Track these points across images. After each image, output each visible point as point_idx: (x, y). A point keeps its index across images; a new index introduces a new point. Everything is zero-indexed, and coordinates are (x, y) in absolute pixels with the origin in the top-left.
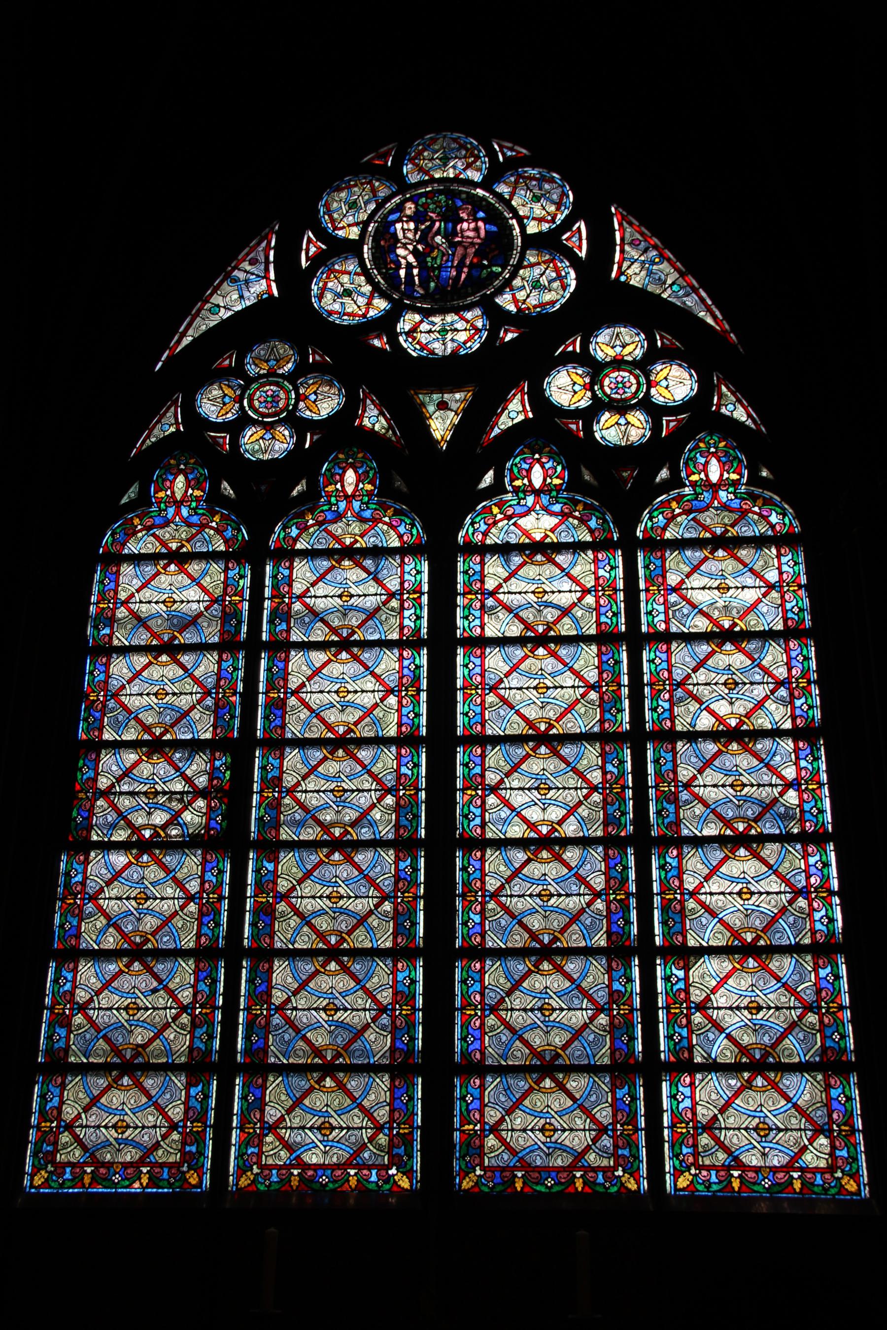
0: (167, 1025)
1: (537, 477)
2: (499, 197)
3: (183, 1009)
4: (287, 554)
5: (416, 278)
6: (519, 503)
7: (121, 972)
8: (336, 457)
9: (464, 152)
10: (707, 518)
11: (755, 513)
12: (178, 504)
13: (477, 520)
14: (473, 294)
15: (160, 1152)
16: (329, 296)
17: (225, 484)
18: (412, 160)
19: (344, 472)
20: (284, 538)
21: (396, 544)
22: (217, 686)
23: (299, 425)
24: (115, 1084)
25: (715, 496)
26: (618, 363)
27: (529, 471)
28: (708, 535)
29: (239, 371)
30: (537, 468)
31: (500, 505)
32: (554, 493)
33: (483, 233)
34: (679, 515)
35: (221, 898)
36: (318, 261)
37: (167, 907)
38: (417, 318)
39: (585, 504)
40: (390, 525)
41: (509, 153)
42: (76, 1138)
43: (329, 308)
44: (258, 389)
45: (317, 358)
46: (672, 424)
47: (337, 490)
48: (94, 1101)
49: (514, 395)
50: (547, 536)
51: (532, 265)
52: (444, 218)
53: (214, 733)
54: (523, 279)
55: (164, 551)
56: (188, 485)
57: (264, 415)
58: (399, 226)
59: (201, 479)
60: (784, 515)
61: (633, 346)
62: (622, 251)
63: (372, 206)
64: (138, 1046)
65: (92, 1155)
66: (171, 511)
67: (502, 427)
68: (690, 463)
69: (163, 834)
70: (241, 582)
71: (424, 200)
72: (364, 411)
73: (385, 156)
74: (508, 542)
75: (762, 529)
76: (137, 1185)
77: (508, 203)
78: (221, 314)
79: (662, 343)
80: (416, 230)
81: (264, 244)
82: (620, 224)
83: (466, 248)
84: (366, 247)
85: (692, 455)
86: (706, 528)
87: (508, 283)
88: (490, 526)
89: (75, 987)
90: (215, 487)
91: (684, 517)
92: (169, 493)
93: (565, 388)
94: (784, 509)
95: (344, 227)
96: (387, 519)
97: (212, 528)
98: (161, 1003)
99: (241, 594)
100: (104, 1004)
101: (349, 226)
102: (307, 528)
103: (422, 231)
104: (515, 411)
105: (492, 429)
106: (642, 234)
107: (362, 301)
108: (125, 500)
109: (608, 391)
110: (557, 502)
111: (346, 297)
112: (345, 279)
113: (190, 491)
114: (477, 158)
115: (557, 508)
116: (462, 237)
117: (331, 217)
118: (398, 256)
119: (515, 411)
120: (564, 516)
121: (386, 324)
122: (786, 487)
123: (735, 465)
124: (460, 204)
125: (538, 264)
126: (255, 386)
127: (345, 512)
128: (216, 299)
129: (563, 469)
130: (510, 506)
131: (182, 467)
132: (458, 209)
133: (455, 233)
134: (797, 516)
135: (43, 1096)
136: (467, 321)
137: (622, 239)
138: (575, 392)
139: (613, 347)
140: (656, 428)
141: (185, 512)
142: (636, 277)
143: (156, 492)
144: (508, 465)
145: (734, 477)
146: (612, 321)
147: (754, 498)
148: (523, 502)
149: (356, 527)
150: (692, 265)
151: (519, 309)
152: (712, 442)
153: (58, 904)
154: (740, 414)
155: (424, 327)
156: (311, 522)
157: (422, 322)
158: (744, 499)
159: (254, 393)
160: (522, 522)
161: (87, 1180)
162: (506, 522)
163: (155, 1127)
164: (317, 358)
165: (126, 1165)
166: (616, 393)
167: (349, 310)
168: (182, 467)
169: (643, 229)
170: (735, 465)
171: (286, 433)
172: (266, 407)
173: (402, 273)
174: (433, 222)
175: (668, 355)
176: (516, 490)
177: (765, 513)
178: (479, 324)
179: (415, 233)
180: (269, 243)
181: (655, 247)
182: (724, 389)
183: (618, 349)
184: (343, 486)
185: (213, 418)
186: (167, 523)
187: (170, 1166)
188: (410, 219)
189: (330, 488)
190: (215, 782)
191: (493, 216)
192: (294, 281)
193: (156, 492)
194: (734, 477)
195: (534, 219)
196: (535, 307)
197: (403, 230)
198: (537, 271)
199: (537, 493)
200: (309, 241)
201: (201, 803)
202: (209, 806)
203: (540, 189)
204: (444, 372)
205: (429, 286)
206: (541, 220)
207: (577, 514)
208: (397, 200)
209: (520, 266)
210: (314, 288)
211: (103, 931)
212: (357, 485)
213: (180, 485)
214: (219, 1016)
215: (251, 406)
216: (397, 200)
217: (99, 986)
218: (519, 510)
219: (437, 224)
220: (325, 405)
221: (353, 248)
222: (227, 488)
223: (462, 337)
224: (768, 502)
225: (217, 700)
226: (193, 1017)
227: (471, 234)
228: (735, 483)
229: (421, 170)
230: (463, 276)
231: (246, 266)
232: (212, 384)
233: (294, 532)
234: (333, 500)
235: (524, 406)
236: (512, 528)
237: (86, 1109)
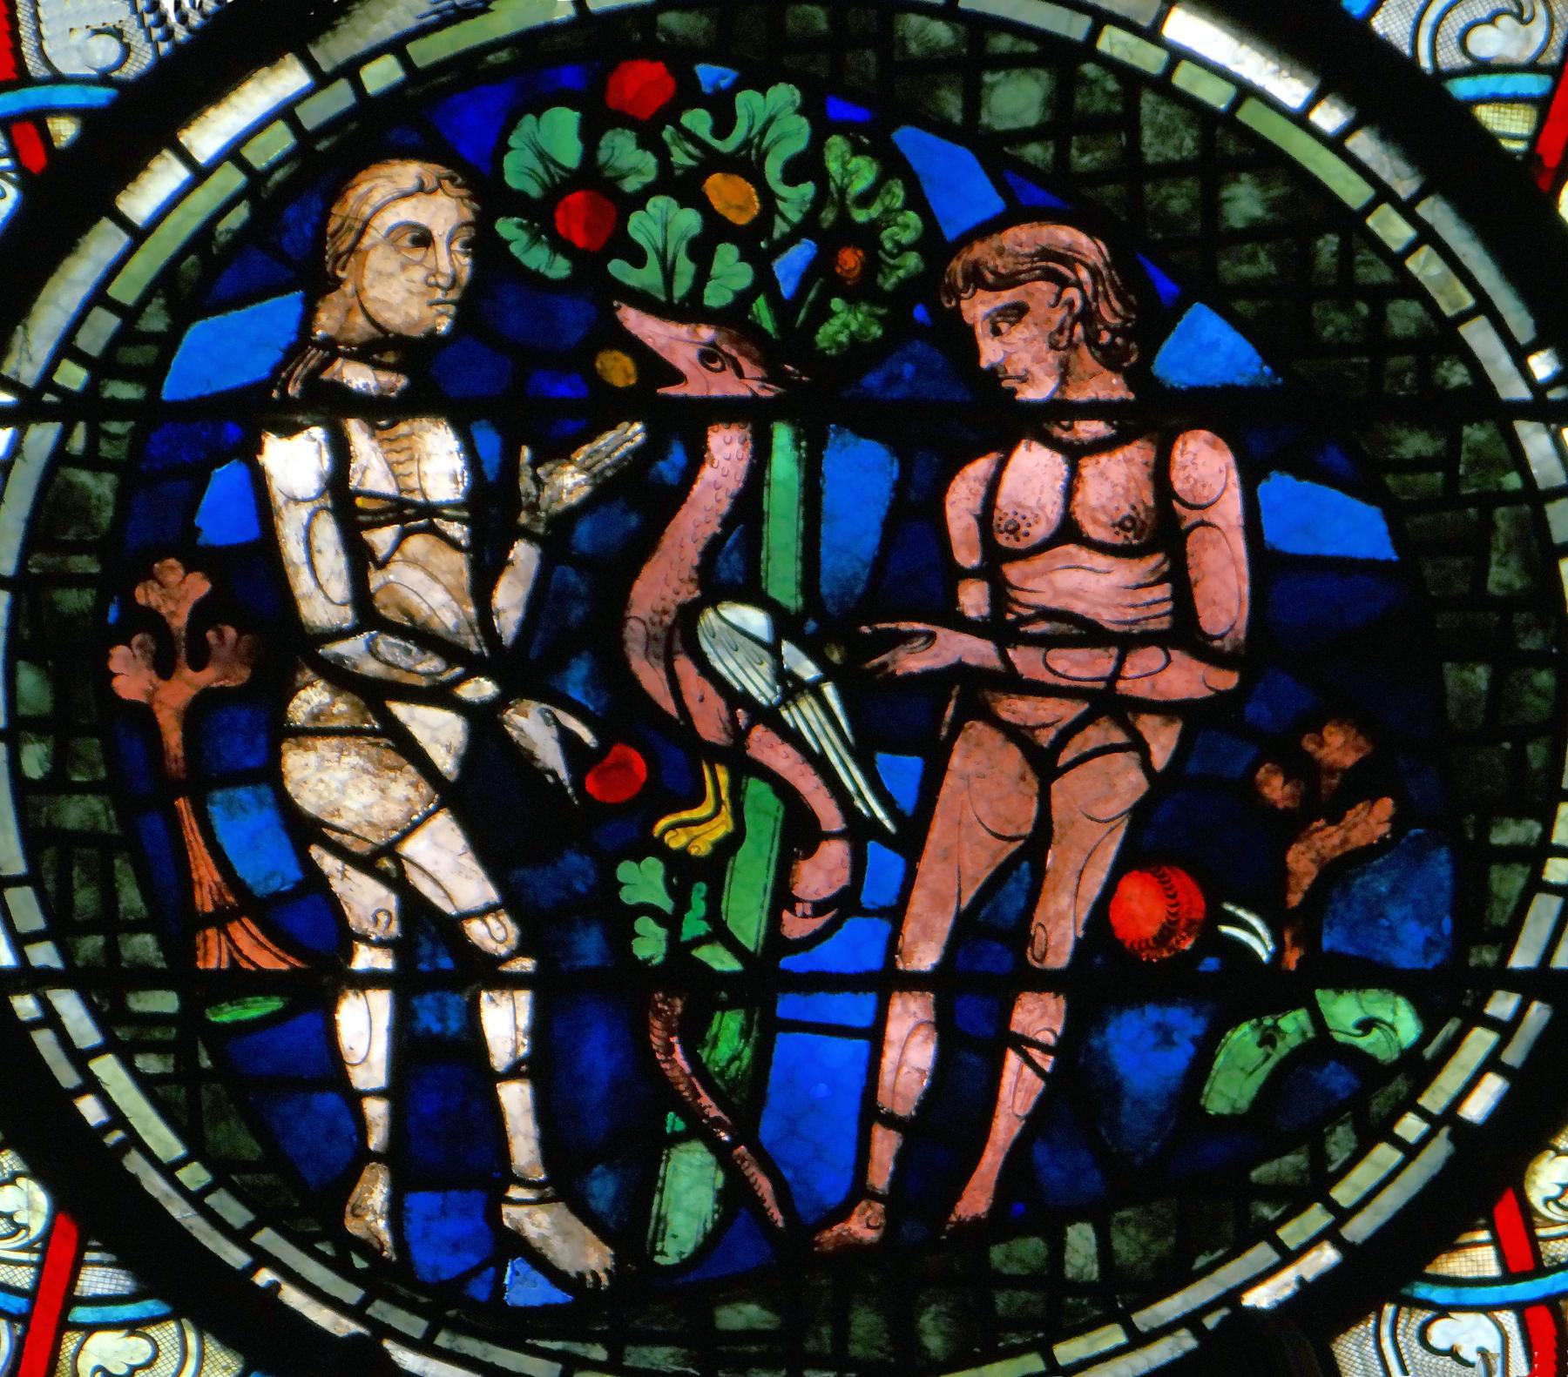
5: (515, 1098)
33: (1225, 591)
52: (813, 395)
58: (294, 462)
71: (558, 133)
80: (491, 514)
83: (1045, 764)
103: (557, 536)
116: (1001, 627)
118: (305, 830)
124: (968, 192)
173: (364, 1028)
174: (686, 426)
179: (486, 570)
188: (430, 377)
205: (643, 1186)
219: (727, 449)
227: (1096, 586)
230: (1018, 1088)
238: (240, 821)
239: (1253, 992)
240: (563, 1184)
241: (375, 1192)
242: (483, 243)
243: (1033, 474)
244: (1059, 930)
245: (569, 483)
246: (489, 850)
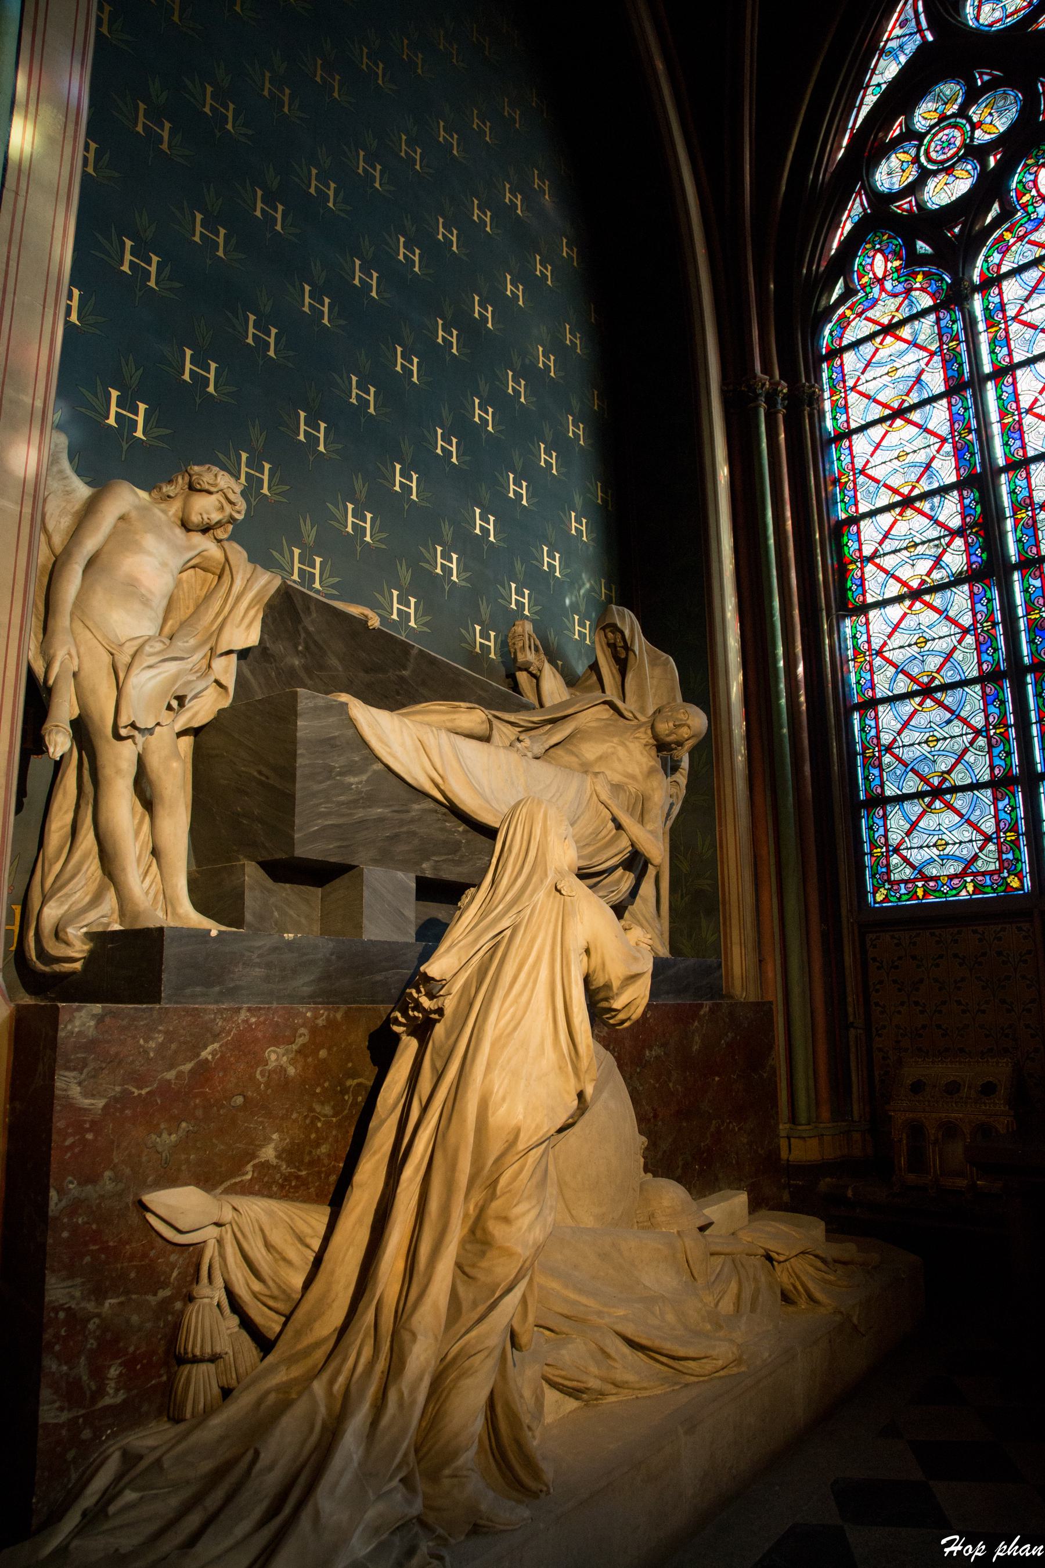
0: (965, 751)
3: (978, 732)
4: (992, 281)
7: (916, 711)
8: (1026, 165)
12: (881, 281)
15: (979, 863)
17: (920, 244)
20: (988, 269)
22: (952, 430)
24: (928, 809)
35: (994, 625)
37: (944, 645)
42: (905, 860)
44: (932, 140)
48: (914, 825)
53: (958, 475)
56: (886, 260)
64: (943, 772)
65: (920, 872)
66: (876, 290)
69: (929, 581)
70: (955, 327)
76: (964, 893)
89: (878, 732)
90: (911, 248)
98: (957, 731)
99: (956, 338)
100: (907, 741)
126: (928, 138)
135: (870, 828)
153: (851, 663)
156: (1012, 241)
161: (920, 893)
163: (971, 841)
165: (951, 877)
186: (875, 302)
187: (991, 873)
190: (968, 520)
201: (959, 542)
202: (966, 543)
211: (893, 680)
214: (1012, 732)
215: (930, 159)
217: (899, 726)
222: (922, 247)
225: (954, 443)
226: (989, 738)
233: (996, 257)
237: (908, 833)
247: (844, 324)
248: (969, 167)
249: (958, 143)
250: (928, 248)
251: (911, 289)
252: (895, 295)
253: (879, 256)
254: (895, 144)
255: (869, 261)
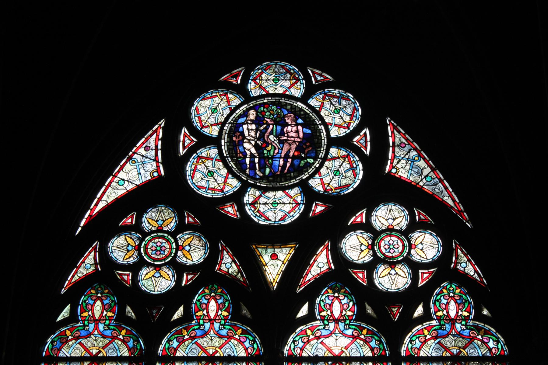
1: (337, 311)
2: (312, 108)
5: (257, 165)
6: (324, 328)
9: (289, 76)
10: (448, 342)
11: (479, 340)
13: (297, 339)
14: (295, 178)
16: (198, 175)
17: (128, 309)
18: (254, 80)
19: (209, 302)
20: (168, 348)
21: (243, 354)
23: (180, 269)
25: (453, 327)
26: (390, 231)
27: (331, 305)
28: (448, 354)
29: (137, 227)
30: (336, 303)
31: (312, 329)
32: (347, 322)
33: (301, 135)
34: (430, 339)
36: (192, 150)
38: (258, 193)
39: (368, 330)
40: (239, 341)
41: (319, 78)
43: (199, 184)
44: (150, 241)
45: (191, 220)
46: (425, 276)
47: (204, 315)
49: (322, 251)
50: (343, 352)
51: (333, 159)
52: (276, 123)
54: (328, 168)
55: (87, 355)
57: (155, 260)
58: (245, 127)
59: (113, 304)
60: (498, 342)
61: (400, 219)
62: (394, 152)
63: (227, 112)
67: (314, 273)
68: (437, 303)
71: (262, 109)
72: (222, 259)
73: (236, 76)
74: (317, 356)
75: (483, 351)
77: (318, 113)
78: (125, 185)
79: (420, 218)
80: (257, 130)
81: (154, 136)
82: (393, 132)
83: (290, 145)
84: (223, 141)
85: (438, 298)
86: (447, 349)
87: (318, 170)
88: (305, 343)
91: (433, 341)
92: (90, 313)
93: (355, 246)
94: (498, 338)
95: (208, 126)
96: (237, 337)
97: (120, 339)
101: (212, 125)
102: (184, 341)
104: (321, 262)
105: (307, 275)
106: (407, 140)
107: (221, 180)
108: (60, 318)
109: (383, 250)
110: (350, 328)
111: (208, 176)
112: (209, 163)
113: (105, 313)
114: (298, 80)
115: (349, 332)
116: (287, 137)
117: (199, 117)
118: (244, 148)
119: (321, 262)
120: (354, 338)
121: (237, 198)
122: (500, 323)
123: (466, 306)
124: (286, 112)
125: (338, 158)
126: (148, 238)
127: (209, 330)
128: (122, 175)
129: (354, 305)
130: (319, 330)
131: (99, 295)
132: (285, 116)
133: (282, 133)
134: (507, 343)
136: (291, 197)
137: (394, 143)
138: (362, 251)
139: (387, 220)
140: (415, 278)
141: (101, 327)
142: (403, 172)
143: (81, 313)
144: (318, 301)
145: (466, 314)
146: (386, 200)
147: (478, 329)
148: (327, 327)
149: (217, 342)
150: (439, 163)
151: (326, 190)
152: (451, 289)
154: (470, 270)
155: (262, 200)
156: (186, 337)
157: (260, 196)
158: (472, 330)
159: (148, 243)
160: (326, 341)
162: (316, 341)
164: (191, 220)
166: (390, 252)
167: (212, 186)
168: (99, 295)
169: (407, 136)
170: (466, 306)
171: (170, 273)
172: (156, 254)
173: (248, 160)
174: (269, 125)
175: (423, 226)
176: (323, 319)
177: (485, 340)
178: (299, 199)
180: (158, 136)
181: (415, 149)
182: (459, 251)
183: (390, 221)
184: (208, 312)
185: (120, 260)
188: (253, 122)
189: (199, 313)
191: (308, 123)
192: (174, 163)
193: (81, 313)
194: (466, 314)
195: (335, 125)
196: (336, 189)
197: (248, 130)
198: (337, 162)
199: (337, 321)
200: (185, 135)
203: (340, 104)
204: (276, 235)
205: (265, 171)
206: (339, 126)
207: (362, 337)
208: (244, 107)
209: (325, 159)
210: (188, 168)
212: (217, 312)
213: (98, 308)
215: (146, 253)
216: (244, 107)
218: (324, 333)
219: (271, 126)
220: (196, 254)
221: (215, 142)
223: (288, 208)
224: (487, 332)
227: (294, 135)
228: (466, 318)
229: (261, 87)
230: (288, 165)
231: (142, 151)
232: (119, 236)
233: (175, 344)
234: (201, 322)
235: (328, 259)
236: (320, 345)
238: (241, 148)
239: (303, 159)
240: (260, 170)
241: (248, 170)
242: (257, 114)
243: (289, 128)
244: (291, 154)
245: (262, 128)
246: (256, 150)
247: (64, 341)
248: (170, 273)
249: (166, 253)
250: (133, 314)
251: (116, 338)
252: (104, 337)
253: (99, 303)
254: (127, 229)
255: (91, 302)
